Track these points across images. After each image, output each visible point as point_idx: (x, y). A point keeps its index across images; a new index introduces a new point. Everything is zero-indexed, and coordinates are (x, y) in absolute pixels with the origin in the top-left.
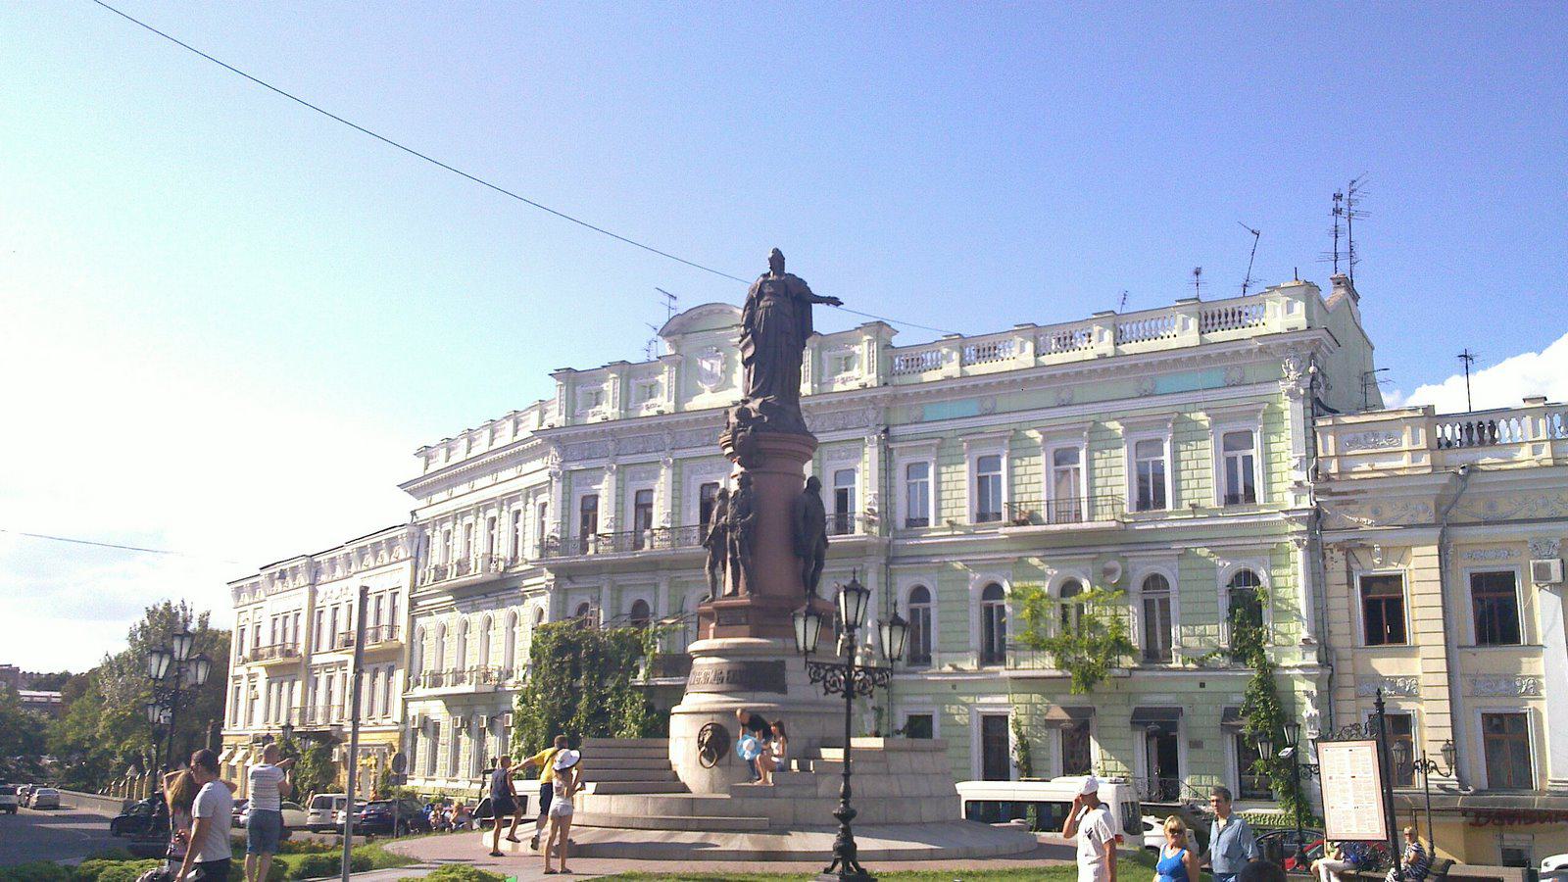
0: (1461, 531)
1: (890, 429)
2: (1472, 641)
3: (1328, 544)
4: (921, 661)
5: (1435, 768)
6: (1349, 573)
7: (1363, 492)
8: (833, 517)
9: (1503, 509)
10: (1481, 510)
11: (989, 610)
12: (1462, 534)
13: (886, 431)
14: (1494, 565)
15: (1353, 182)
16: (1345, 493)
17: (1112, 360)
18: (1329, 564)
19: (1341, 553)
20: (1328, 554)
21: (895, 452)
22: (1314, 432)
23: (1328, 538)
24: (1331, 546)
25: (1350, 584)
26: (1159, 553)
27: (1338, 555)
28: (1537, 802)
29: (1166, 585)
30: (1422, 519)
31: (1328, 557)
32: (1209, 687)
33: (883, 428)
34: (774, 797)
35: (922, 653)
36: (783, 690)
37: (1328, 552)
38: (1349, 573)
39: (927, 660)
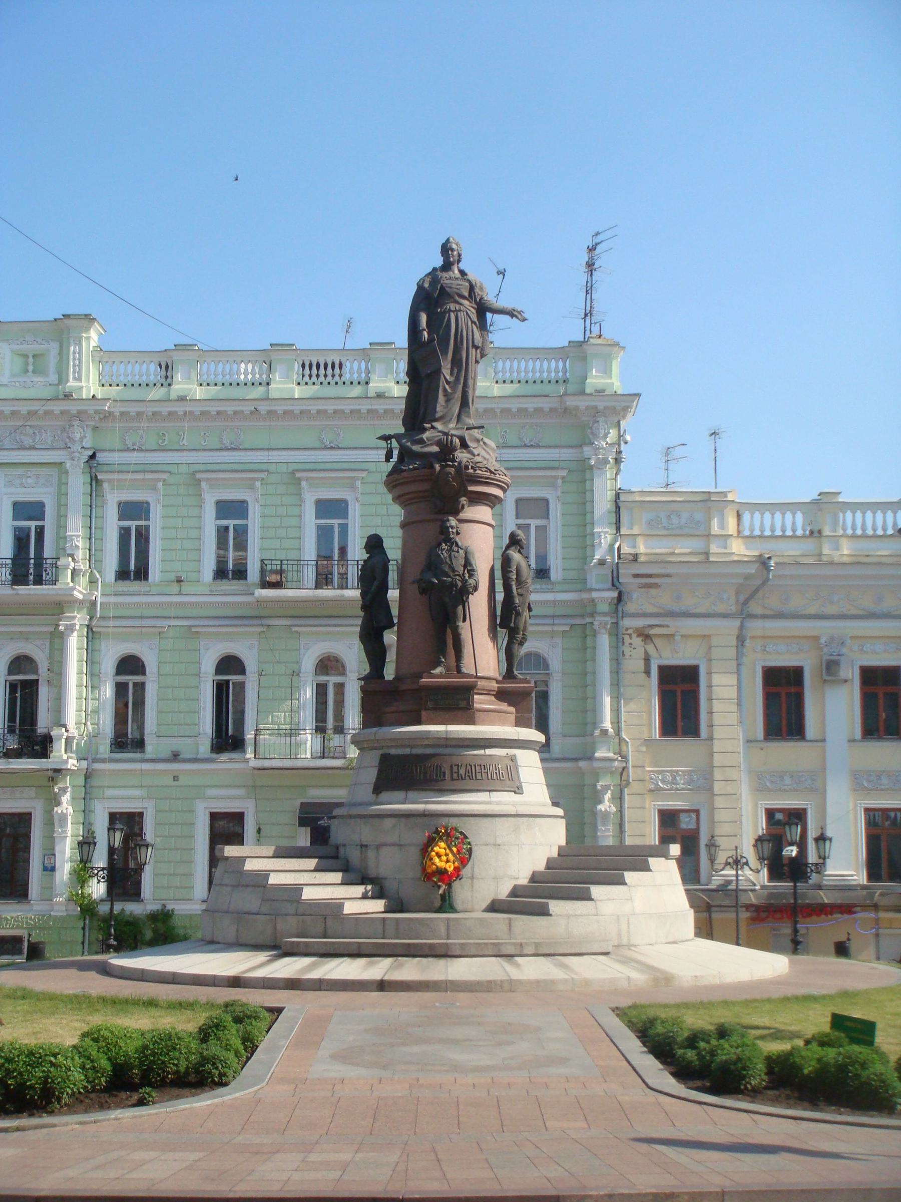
0: (759, 623)
1: (97, 455)
2: (760, 735)
3: (627, 629)
4: (129, 746)
5: (747, 863)
6: (647, 660)
7: (668, 576)
8: (9, 561)
9: (796, 603)
10: (774, 602)
11: (221, 690)
12: (756, 627)
13: (93, 457)
14: (784, 659)
15: (597, 234)
16: (650, 576)
17: (373, 401)
18: (627, 649)
19: (640, 639)
20: (627, 639)
21: (105, 485)
22: (618, 508)
23: (627, 622)
24: (630, 631)
25: (647, 672)
26: (314, 629)
27: (637, 641)
28: (826, 898)
29: (547, 667)
30: (721, 608)
31: (627, 643)
32: (183, 780)
33: (91, 453)
34: (597, 915)
35: (130, 736)
36: (518, 790)
37: (627, 638)
38: (647, 660)
39: (140, 744)
